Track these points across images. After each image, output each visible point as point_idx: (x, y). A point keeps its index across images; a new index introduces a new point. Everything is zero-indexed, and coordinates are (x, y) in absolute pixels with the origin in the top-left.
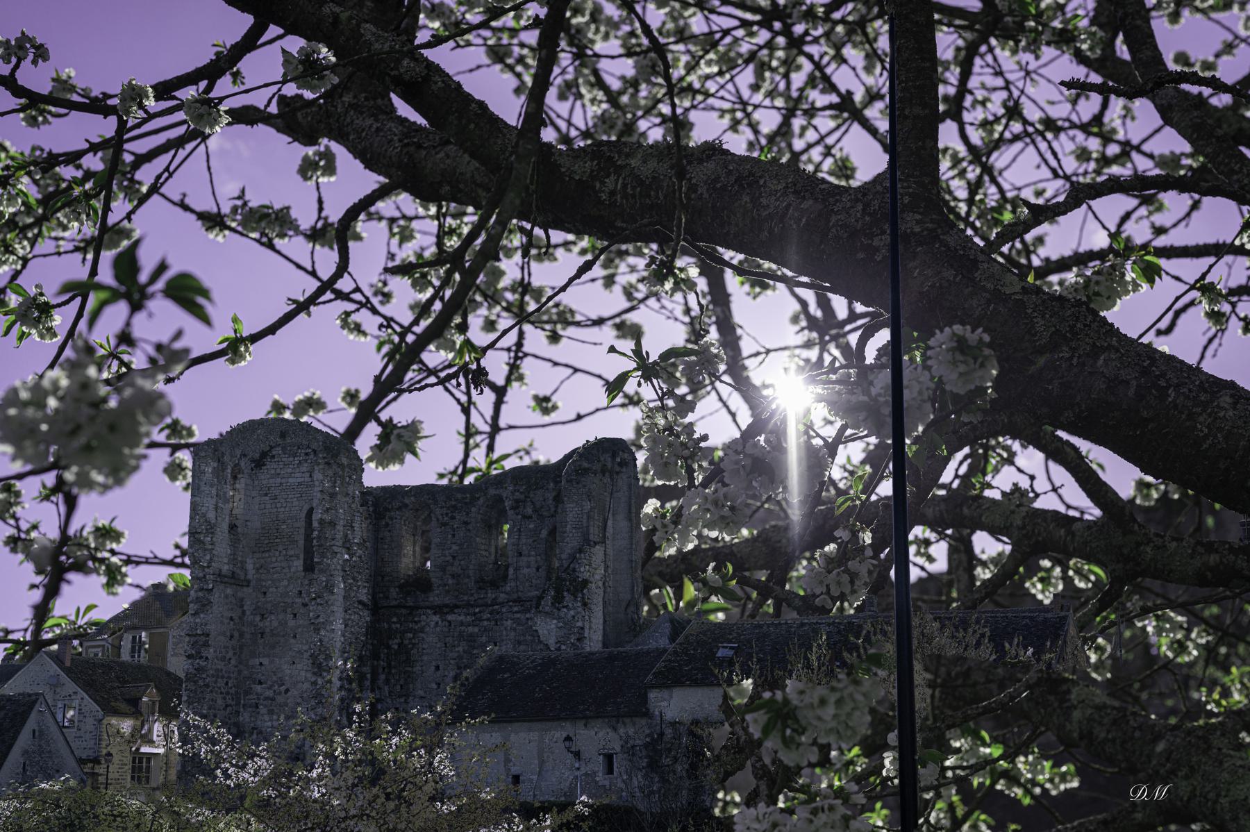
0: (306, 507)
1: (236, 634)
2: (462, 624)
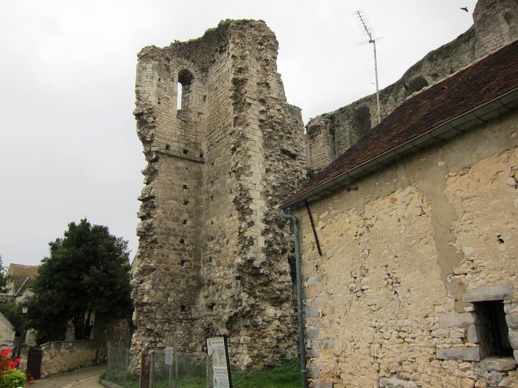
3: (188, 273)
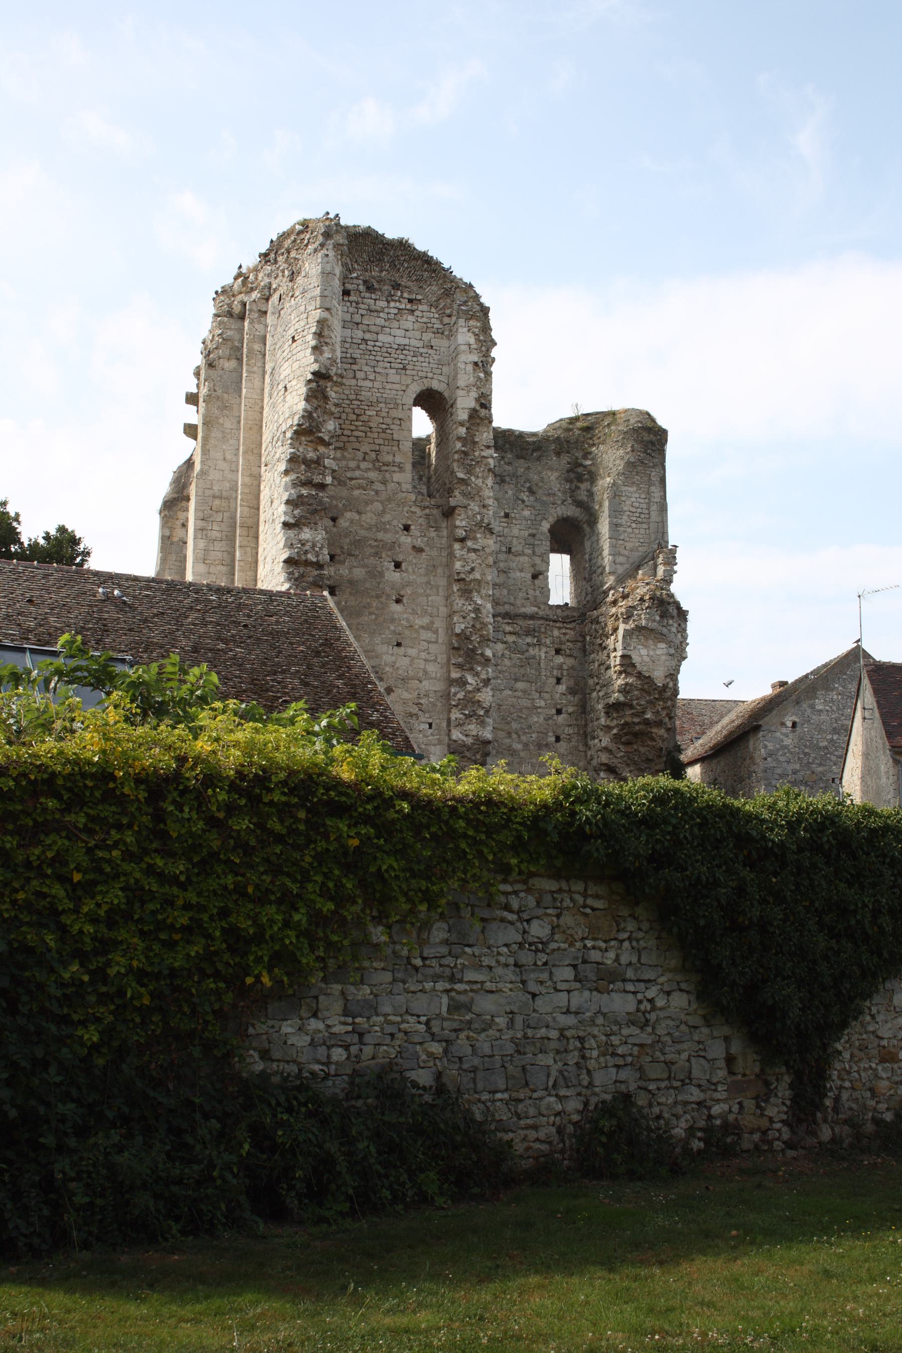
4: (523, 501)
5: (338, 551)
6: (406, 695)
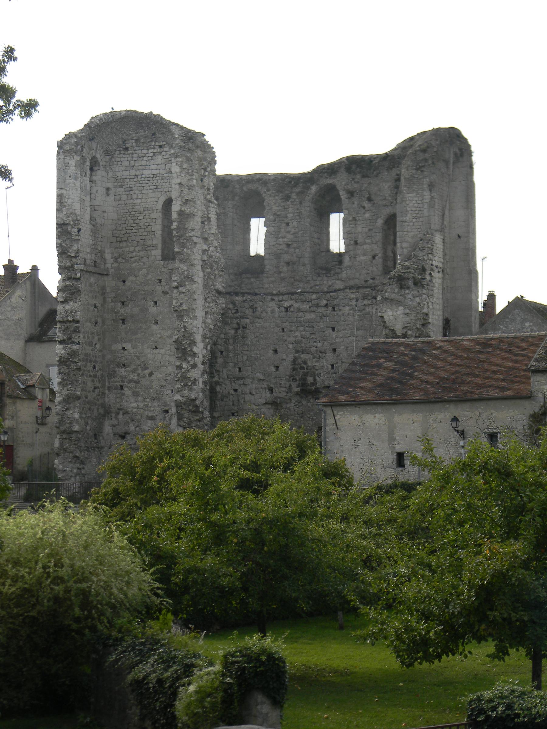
0: (162, 199)
1: (100, 321)
2: (299, 310)
3: (98, 400)
4: (364, 208)
5: (125, 300)
6: (160, 376)
